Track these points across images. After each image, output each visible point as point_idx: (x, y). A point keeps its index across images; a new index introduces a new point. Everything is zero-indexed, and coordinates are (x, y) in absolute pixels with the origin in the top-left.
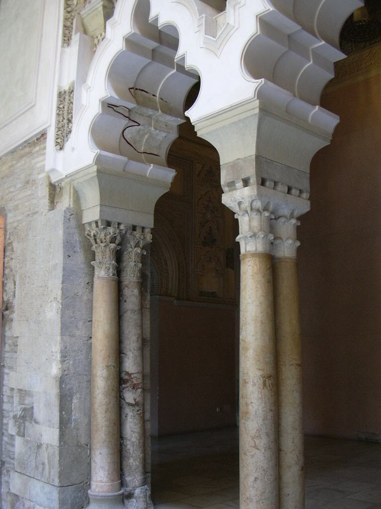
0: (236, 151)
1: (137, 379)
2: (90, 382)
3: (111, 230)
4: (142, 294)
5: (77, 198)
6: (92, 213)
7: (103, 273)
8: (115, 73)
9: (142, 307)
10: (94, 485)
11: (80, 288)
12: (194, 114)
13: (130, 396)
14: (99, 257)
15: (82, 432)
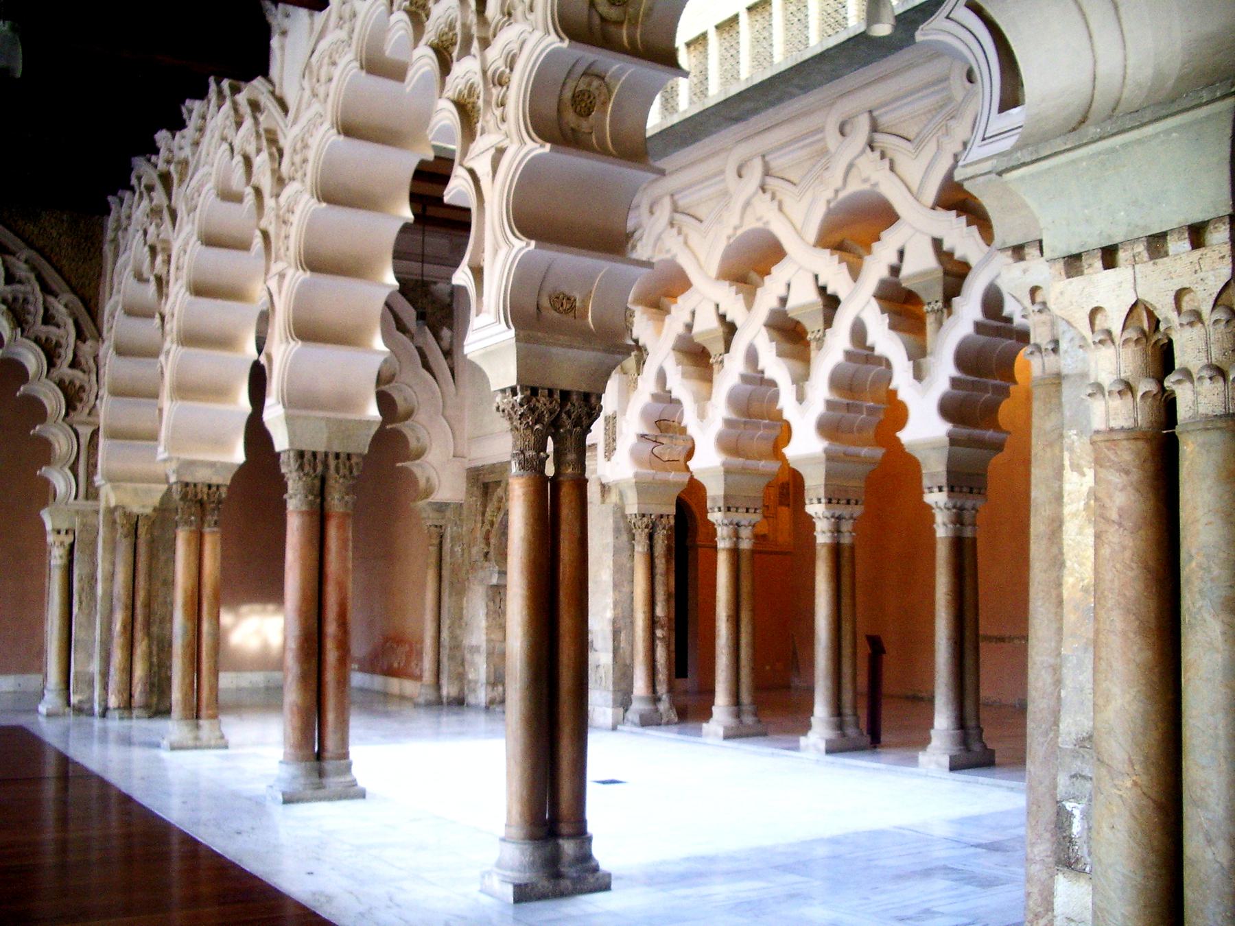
0: (715, 490)
1: (664, 621)
2: (632, 623)
3: (645, 519)
4: (668, 561)
5: (621, 495)
6: (632, 508)
7: (640, 548)
8: (645, 414)
9: (668, 570)
10: (635, 691)
11: (624, 559)
12: (692, 464)
13: (659, 633)
14: (637, 537)
15: (628, 653)
